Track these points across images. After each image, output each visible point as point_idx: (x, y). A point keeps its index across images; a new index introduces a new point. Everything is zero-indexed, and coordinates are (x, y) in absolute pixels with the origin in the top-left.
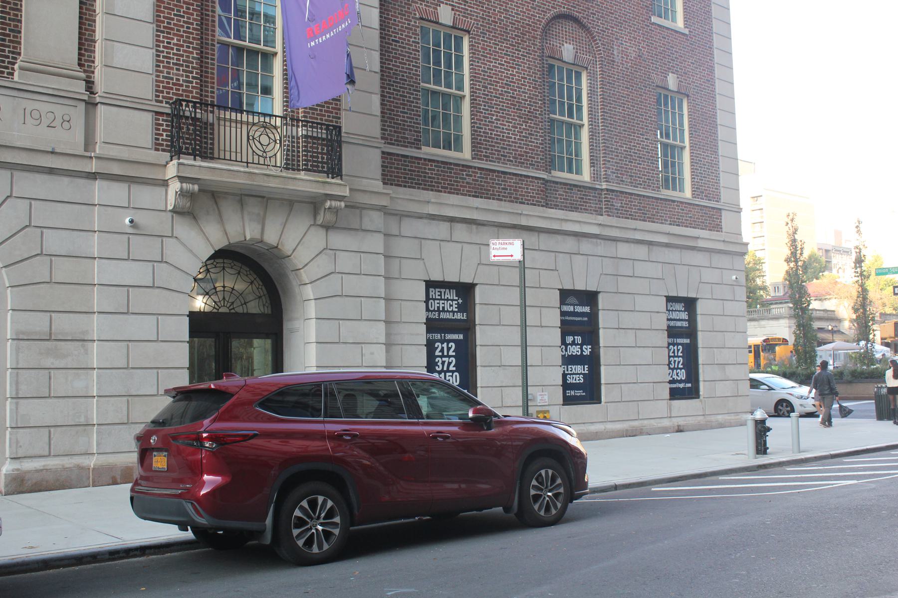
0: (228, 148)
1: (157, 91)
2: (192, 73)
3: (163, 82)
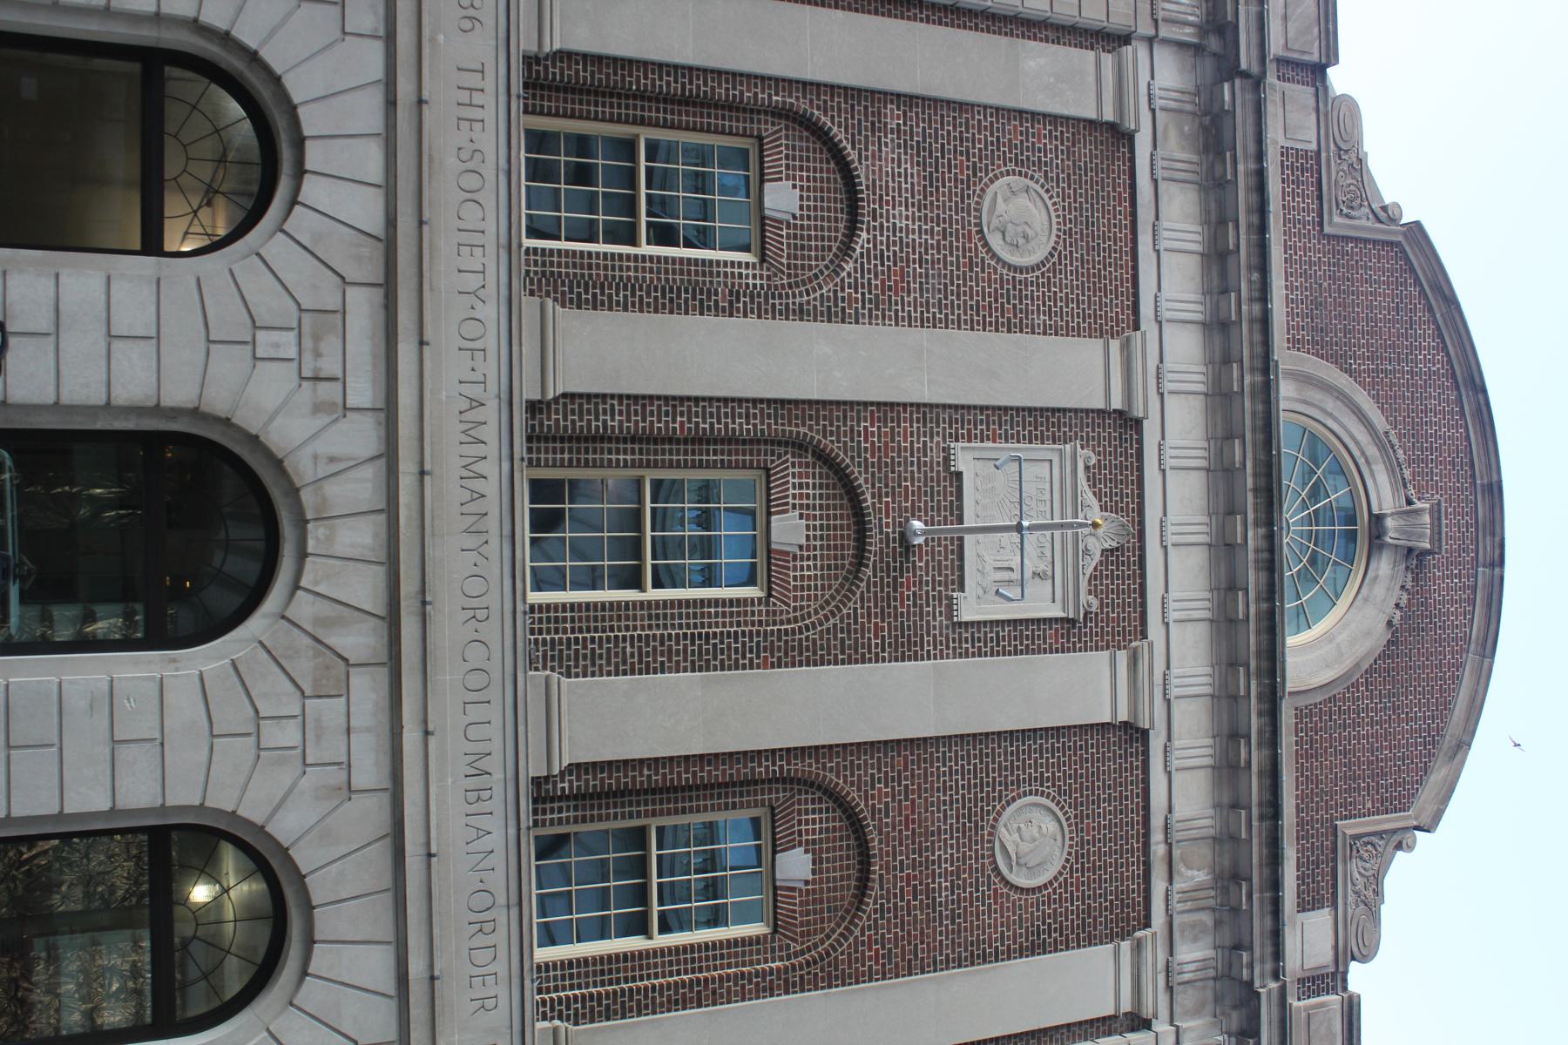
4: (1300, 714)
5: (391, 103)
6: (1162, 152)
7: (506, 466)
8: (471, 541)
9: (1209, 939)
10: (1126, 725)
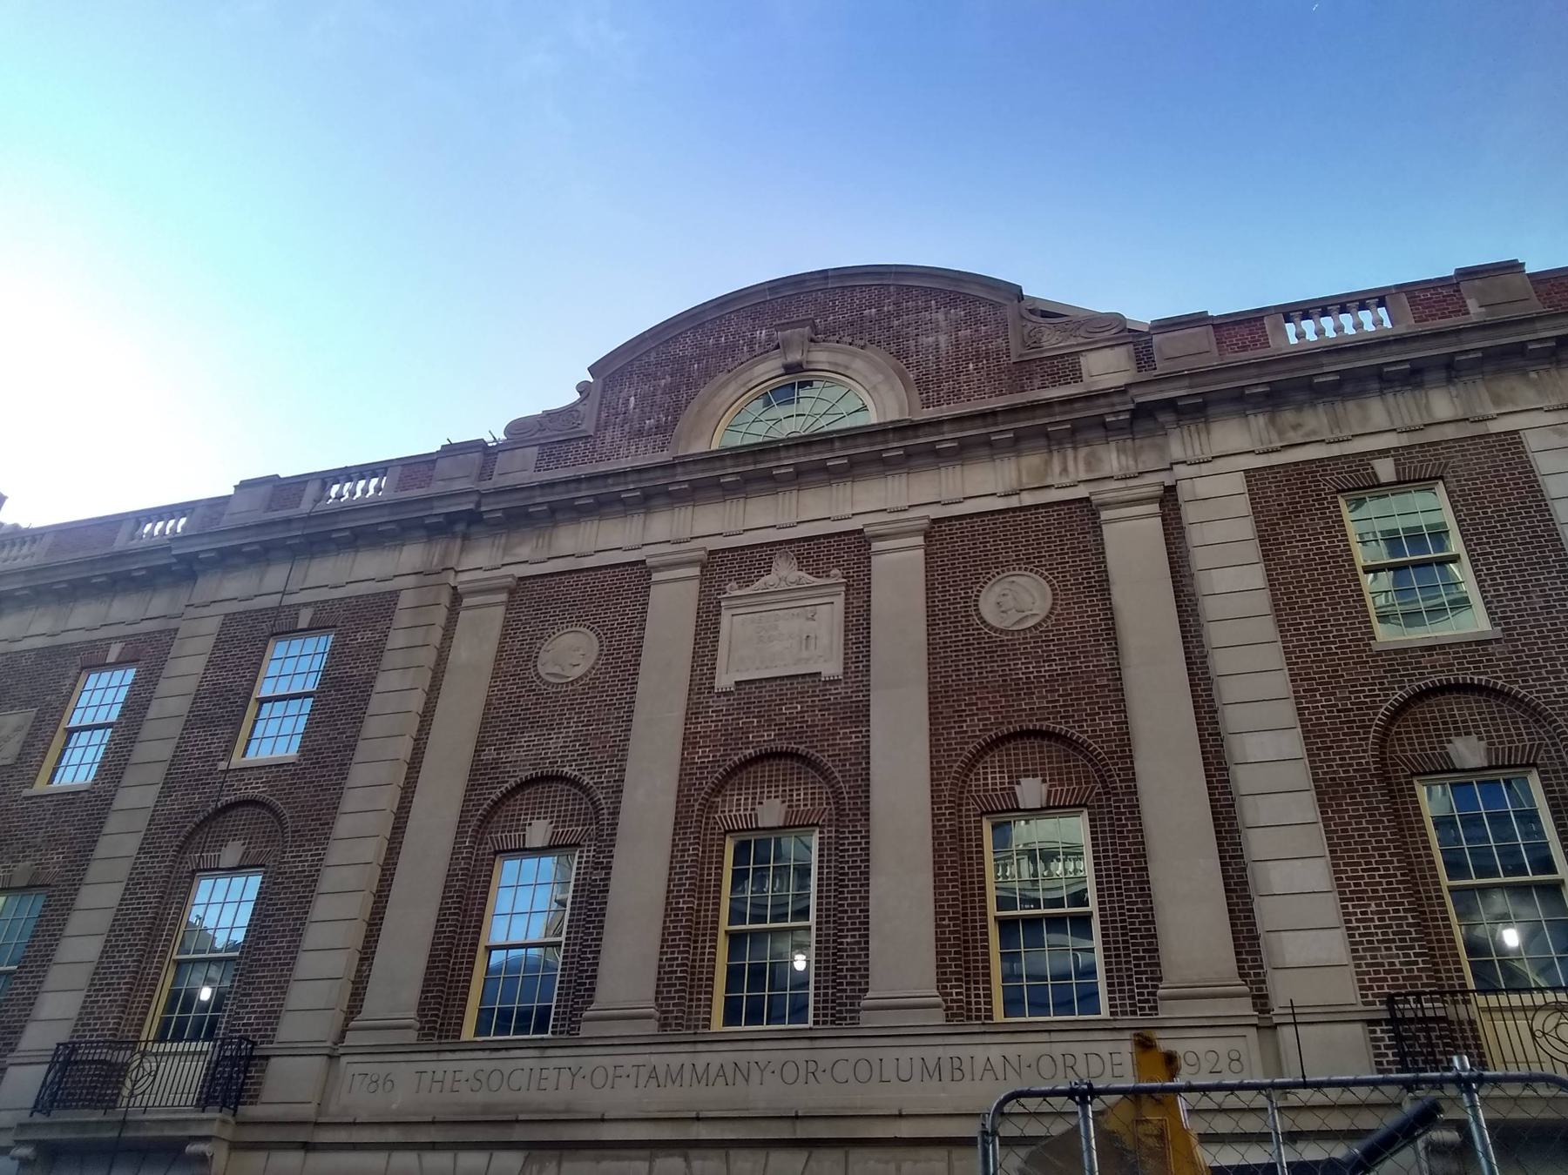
0: (1521, 1057)
1: (1361, 988)
2: (1412, 948)
3: (1368, 973)
4: (926, 404)
5: (433, 1146)
6: (530, 555)
7: (700, 1047)
8: (755, 1076)
9: (1100, 448)
10: (927, 536)
